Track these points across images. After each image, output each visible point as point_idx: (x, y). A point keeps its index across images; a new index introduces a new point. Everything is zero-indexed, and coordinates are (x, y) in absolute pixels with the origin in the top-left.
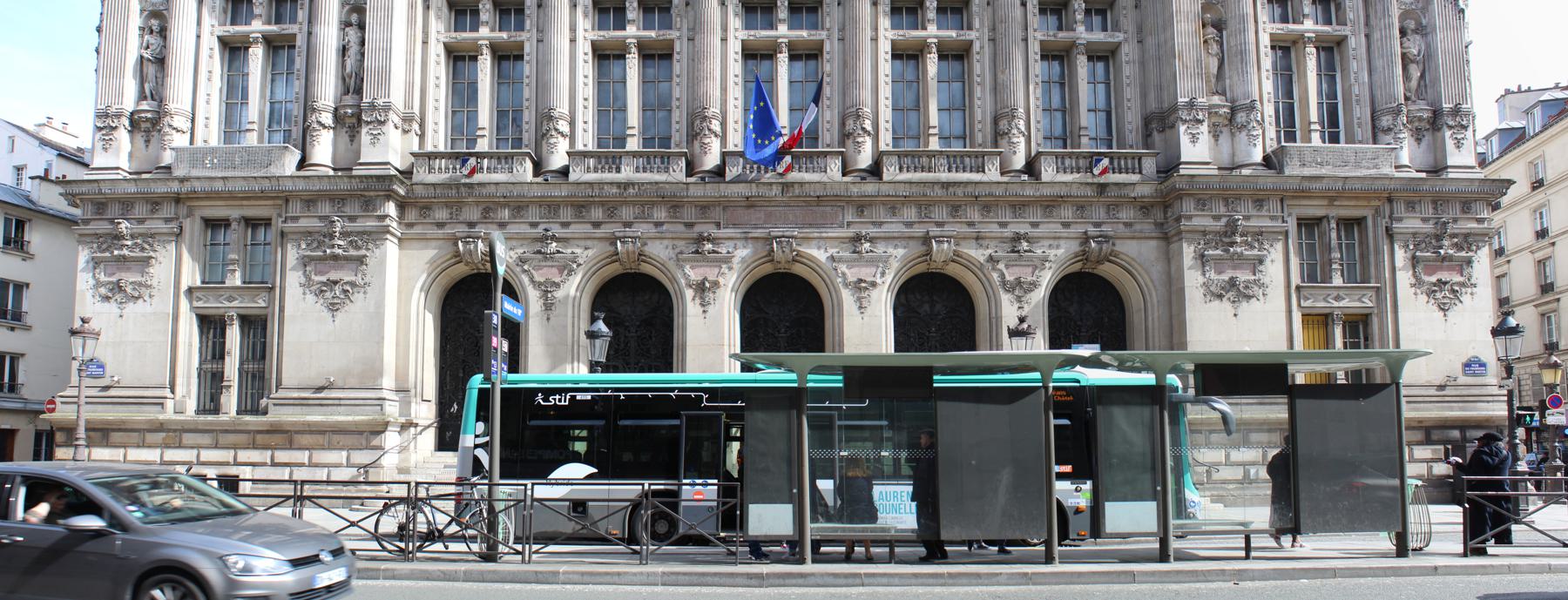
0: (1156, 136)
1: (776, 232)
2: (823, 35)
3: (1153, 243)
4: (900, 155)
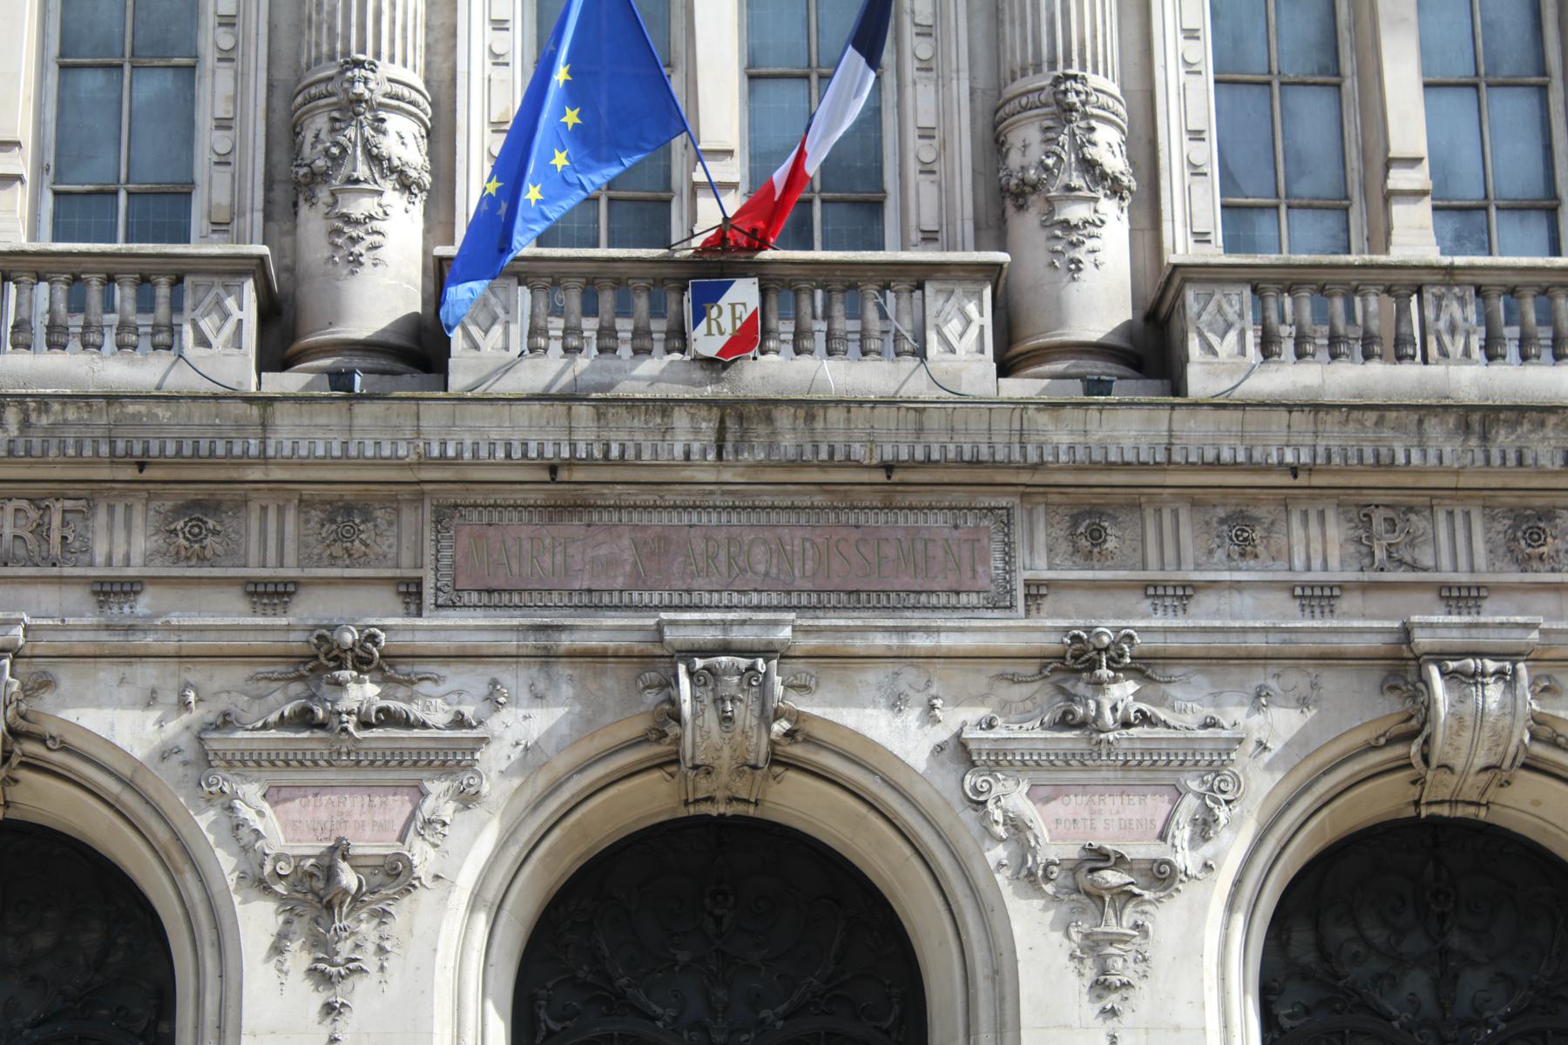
1: (689, 627)
4: (1260, 284)
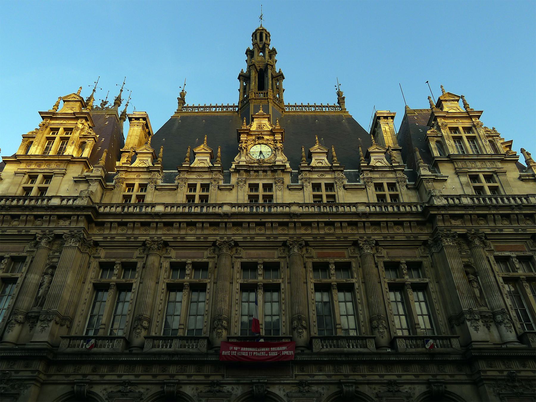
0: (457, 328)
2: (281, 281)
3: (468, 387)
